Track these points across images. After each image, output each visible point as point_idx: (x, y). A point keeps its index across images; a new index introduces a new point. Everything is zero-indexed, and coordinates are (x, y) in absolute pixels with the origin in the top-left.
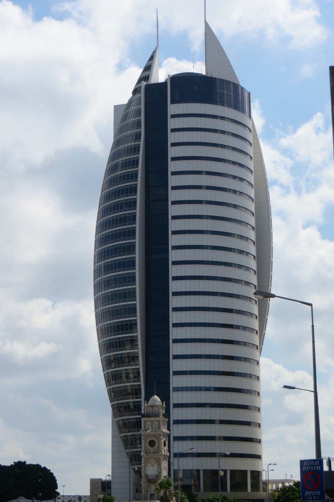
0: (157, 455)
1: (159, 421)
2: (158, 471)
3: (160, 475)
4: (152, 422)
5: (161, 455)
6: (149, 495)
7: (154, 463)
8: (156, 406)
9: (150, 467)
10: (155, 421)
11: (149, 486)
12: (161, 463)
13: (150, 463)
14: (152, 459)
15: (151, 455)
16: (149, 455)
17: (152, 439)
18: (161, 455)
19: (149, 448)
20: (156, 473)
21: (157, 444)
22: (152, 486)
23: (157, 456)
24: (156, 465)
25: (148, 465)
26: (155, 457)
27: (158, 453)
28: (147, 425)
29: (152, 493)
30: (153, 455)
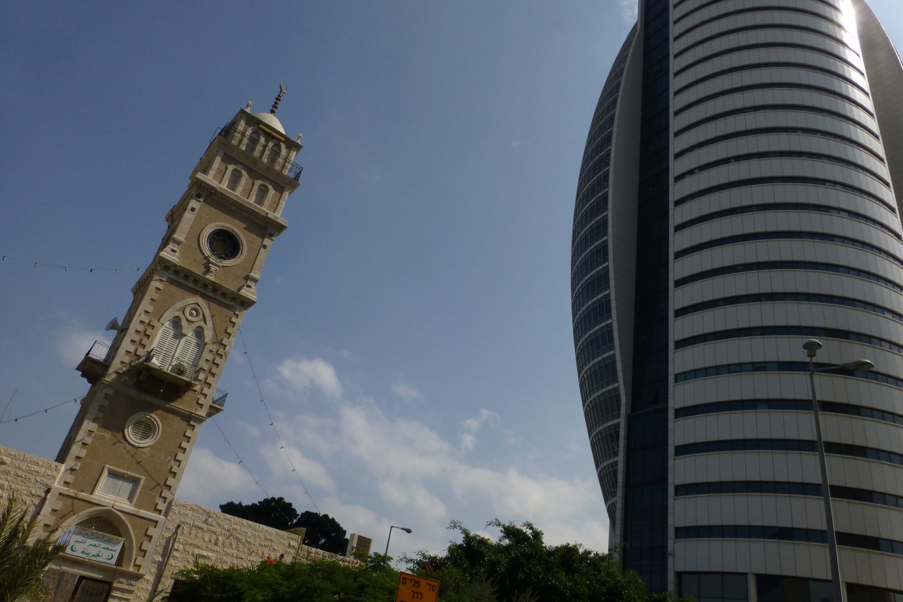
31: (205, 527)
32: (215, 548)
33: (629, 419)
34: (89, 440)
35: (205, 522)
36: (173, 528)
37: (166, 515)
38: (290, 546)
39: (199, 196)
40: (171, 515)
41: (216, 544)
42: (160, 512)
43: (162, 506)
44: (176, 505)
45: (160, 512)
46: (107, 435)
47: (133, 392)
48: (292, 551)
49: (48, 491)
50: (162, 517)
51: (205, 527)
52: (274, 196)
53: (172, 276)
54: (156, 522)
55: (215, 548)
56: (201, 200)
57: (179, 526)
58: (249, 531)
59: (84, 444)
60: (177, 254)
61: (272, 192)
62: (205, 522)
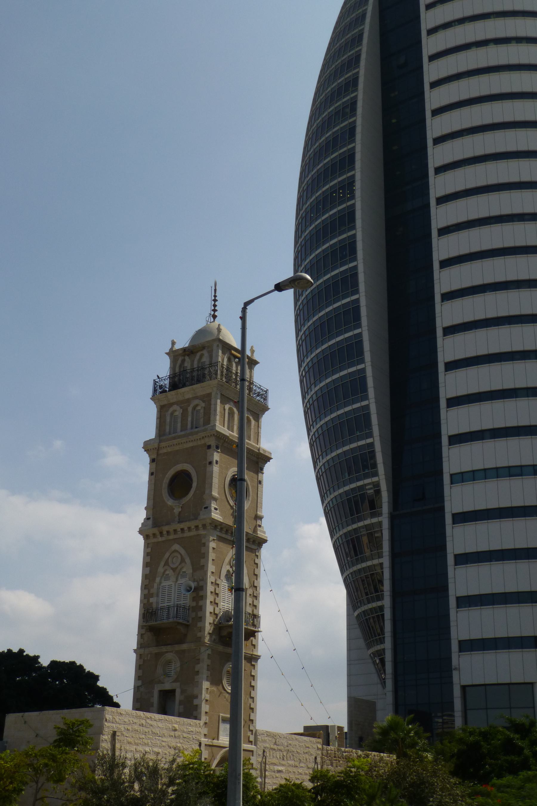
0: (192, 524)
1: (207, 399)
2: (189, 589)
3: (199, 609)
4: (184, 404)
5: (204, 526)
6: (155, 699)
7: (183, 560)
8: (203, 348)
9: (167, 578)
10: (196, 398)
11: (158, 656)
12: (204, 556)
13: (167, 563)
14: (176, 547)
15: (171, 528)
16: (165, 529)
17: (179, 467)
18: (204, 526)
19: (170, 502)
20: (186, 600)
21: (194, 485)
22: (169, 656)
23: (193, 533)
24: (188, 568)
25: (161, 569)
26: (187, 534)
27: (196, 517)
28: (168, 419)
29: (167, 686)
30: (179, 527)
31: (275, 747)
32: (283, 762)
33: (393, 518)
34: (208, 697)
35: (275, 744)
36: (261, 753)
37: (255, 745)
38: (318, 749)
39: (217, 447)
40: (260, 744)
41: (283, 759)
42: (251, 742)
43: (252, 738)
44: (260, 735)
45: (251, 742)
46: (214, 688)
47: (221, 648)
48: (319, 752)
49: (200, 745)
50: (253, 746)
51: (275, 747)
52: (255, 425)
53: (219, 534)
54: (252, 751)
55: (283, 762)
56: (219, 451)
57: (264, 751)
58: (297, 743)
59: (207, 700)
60: (218, 511)
61: (253, 422)
62: (275, 744)
